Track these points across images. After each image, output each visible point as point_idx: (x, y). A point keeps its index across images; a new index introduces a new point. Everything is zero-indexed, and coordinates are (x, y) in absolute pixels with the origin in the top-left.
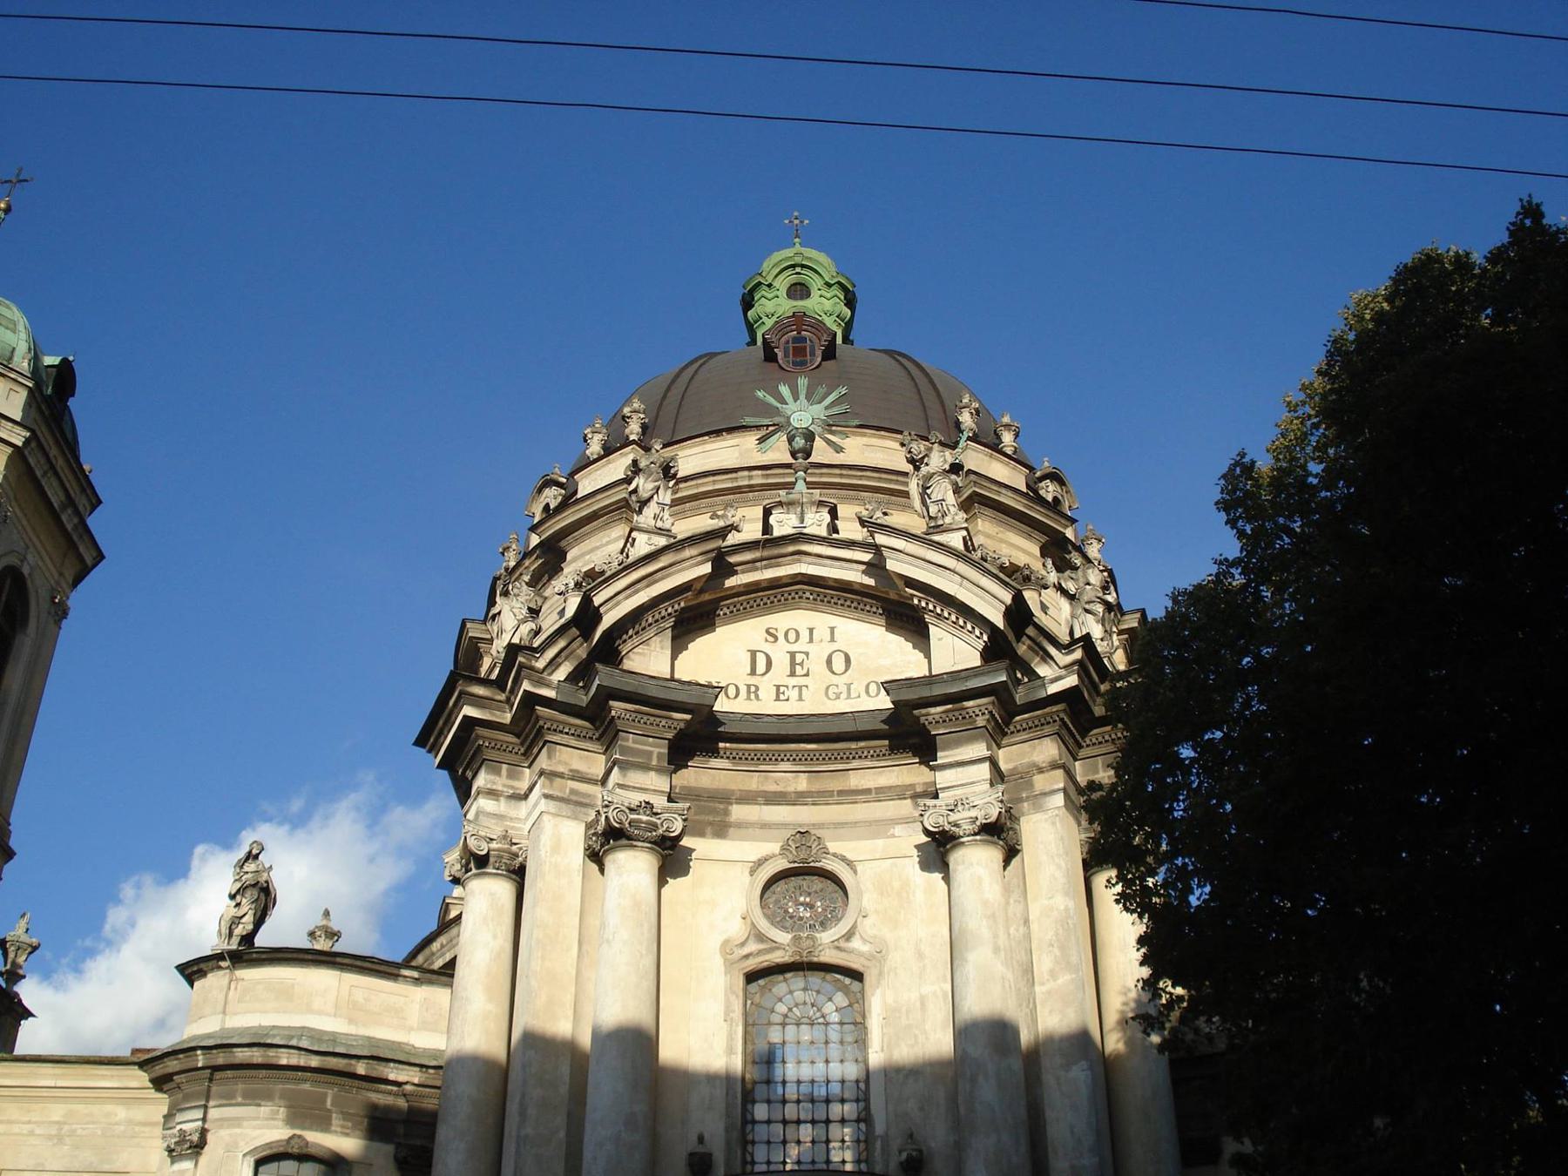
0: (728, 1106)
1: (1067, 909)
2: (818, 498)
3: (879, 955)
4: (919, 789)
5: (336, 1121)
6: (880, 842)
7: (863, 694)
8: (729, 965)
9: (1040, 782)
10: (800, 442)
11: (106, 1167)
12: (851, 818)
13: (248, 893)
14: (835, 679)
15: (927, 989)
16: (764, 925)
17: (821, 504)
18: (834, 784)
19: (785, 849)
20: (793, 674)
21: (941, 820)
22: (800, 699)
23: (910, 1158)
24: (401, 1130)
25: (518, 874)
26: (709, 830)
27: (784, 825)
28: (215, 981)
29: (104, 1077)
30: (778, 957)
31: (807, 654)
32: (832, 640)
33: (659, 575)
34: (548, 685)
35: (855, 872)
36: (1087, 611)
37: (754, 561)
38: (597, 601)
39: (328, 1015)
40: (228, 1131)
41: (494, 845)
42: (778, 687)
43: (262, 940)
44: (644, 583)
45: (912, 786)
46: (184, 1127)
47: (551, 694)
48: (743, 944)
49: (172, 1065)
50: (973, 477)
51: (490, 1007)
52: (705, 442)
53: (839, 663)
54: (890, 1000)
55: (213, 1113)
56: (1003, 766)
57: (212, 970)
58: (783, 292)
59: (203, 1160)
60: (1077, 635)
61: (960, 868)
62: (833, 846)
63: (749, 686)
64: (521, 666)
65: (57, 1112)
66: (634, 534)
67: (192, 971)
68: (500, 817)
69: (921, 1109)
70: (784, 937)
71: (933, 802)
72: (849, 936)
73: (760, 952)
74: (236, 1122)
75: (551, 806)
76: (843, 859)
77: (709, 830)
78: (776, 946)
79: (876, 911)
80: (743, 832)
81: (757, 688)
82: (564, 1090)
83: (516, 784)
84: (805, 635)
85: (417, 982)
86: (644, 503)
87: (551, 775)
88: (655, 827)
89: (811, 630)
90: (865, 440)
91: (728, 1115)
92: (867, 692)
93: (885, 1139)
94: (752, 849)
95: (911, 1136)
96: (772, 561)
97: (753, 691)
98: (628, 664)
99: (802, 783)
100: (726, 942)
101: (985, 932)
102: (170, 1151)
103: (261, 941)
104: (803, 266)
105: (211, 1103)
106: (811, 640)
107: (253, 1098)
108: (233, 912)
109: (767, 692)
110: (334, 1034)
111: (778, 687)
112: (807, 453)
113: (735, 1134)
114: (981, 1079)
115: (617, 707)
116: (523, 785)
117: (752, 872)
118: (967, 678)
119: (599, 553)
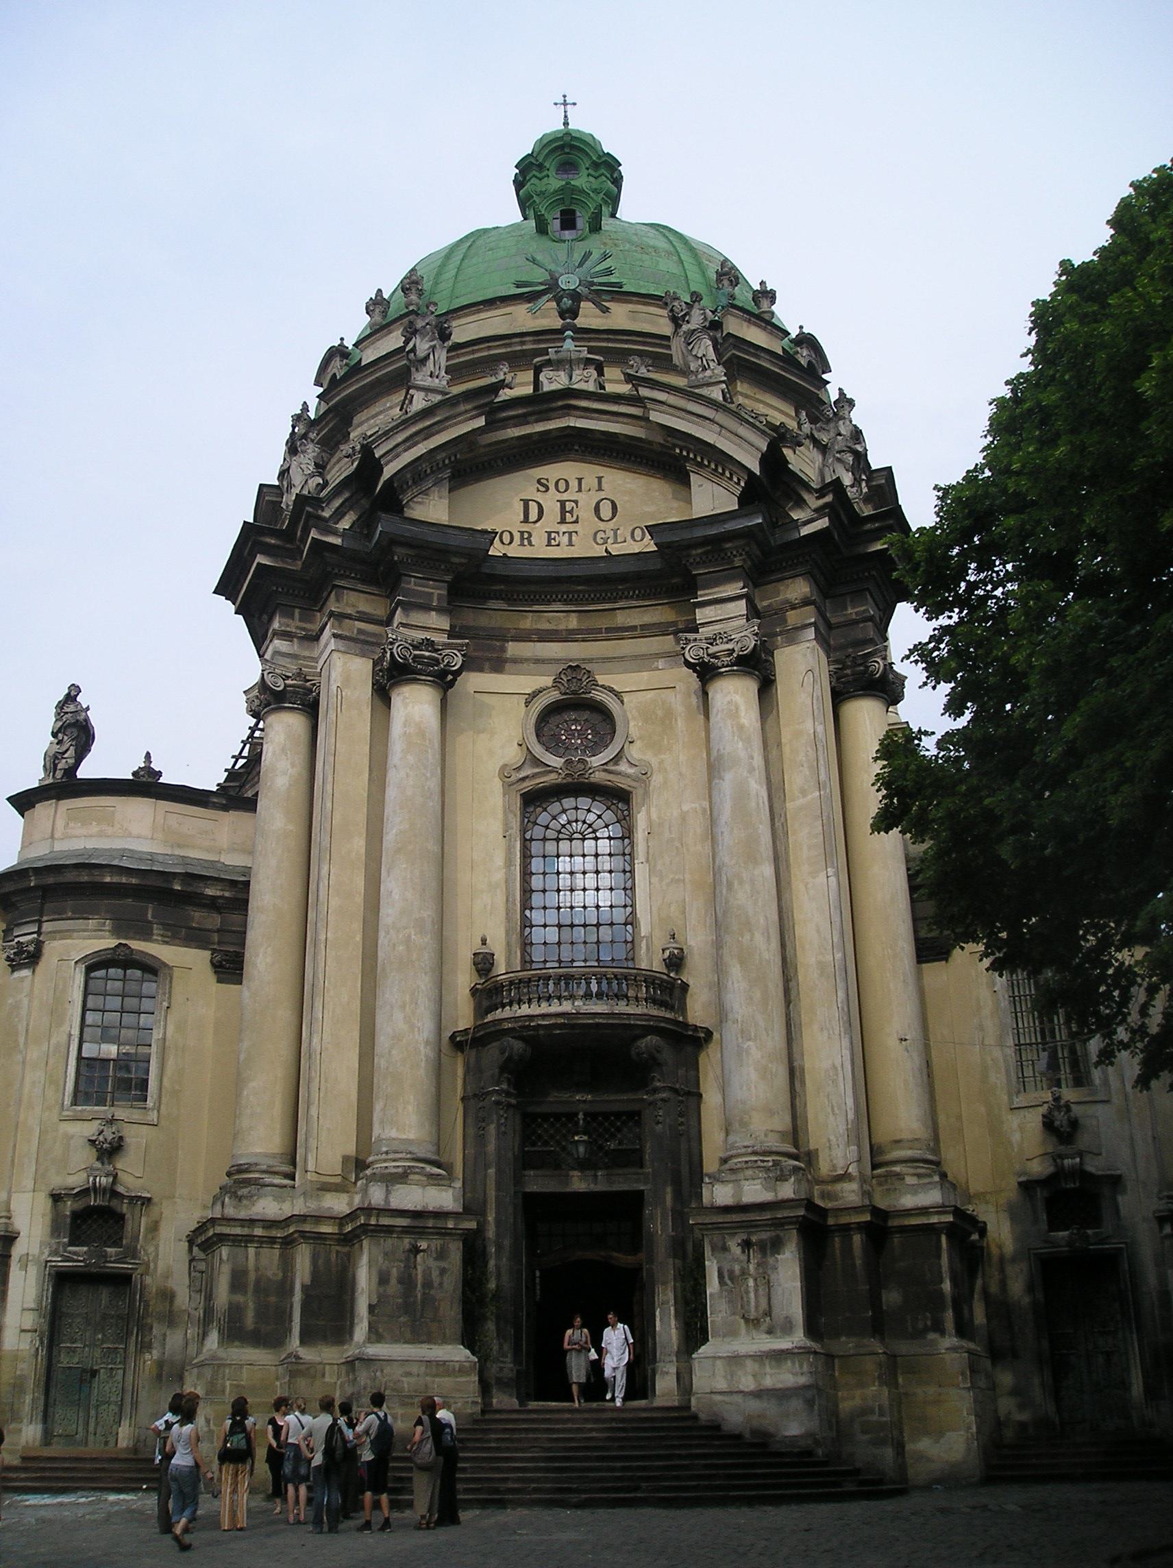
2: (585, 354)
5: (157, 930)
7: (629, 538)
8: (508, 786)
9: (793, 617)
10: (567, 302)
13: (69, 731)
14: (602, 525)
15: (685, 808)
16: (538, 750)
17: (588, 362)
18: (603, 622)
20: (563, 521)
22: (570, 544)
23: (672, 954)
24: (216, 937)
25: (311, 708)
26: (487, 665)
27: (557, 661)
28: (43, 810)
30: (551, 778)
31: (576, 502)
32: (600, 489)
33: (436, 428)
34: (334, 533)
35: (622, 702)
36: (839, 460)
37: (524, 415)
41: (289, 682)
42: (549, 533)
43: (82, 773)
44: (422, 436)
45: (674, 623)
46: (22, 939)
47: (337, 541)
50: (731, 340)
51: (290, 827)
52: (479, 311)
53: (606, 511)
54: (654, 816)
55: (46, 927)
56: (762, 604)
58: (552, 172)
59: (41, 968)
60: (828, 480)
62: (601, 679)
63: (522, 533)
64: (309, 515)
67: (23, 802)
68: (294, 657)
70: (556, 762)
71: (691, 636)
72: (616, 759)
73: (534, 776)
75: (341, 645)
76: (611, 690)
77: (487, 665)
79: (640, 738)
80: (519, 666)
81: (530, 535)
82: (359, 899)
83: (308, 626)
84: (574, 484)
85: (225, 808)
87: (340, 617)
88: (437, 662)
89: (580, 480)
90: (631, 307)
91: (508, 918)
92: (633, 537)
93: (649, 938)
94: (527, 683)
95: (673, 937)
96: (544, 416)
97: (526, 538)
98: (409, 513)
99: (573, 622)
100: (505, 766)
101: (742, 754)
102: (8, 959)
103: (82, 773)
104: (573, 147)
105: (45, 918)
106: (580, 490)
107: (82, 914)
108: (56, 748)
109: (539, 539)
110: (151, 854)
111: (549, 533)
112: (574, 313)
113: (515, 938)
116: (317, 627)
117: (527, 703)
118: (724, 521)
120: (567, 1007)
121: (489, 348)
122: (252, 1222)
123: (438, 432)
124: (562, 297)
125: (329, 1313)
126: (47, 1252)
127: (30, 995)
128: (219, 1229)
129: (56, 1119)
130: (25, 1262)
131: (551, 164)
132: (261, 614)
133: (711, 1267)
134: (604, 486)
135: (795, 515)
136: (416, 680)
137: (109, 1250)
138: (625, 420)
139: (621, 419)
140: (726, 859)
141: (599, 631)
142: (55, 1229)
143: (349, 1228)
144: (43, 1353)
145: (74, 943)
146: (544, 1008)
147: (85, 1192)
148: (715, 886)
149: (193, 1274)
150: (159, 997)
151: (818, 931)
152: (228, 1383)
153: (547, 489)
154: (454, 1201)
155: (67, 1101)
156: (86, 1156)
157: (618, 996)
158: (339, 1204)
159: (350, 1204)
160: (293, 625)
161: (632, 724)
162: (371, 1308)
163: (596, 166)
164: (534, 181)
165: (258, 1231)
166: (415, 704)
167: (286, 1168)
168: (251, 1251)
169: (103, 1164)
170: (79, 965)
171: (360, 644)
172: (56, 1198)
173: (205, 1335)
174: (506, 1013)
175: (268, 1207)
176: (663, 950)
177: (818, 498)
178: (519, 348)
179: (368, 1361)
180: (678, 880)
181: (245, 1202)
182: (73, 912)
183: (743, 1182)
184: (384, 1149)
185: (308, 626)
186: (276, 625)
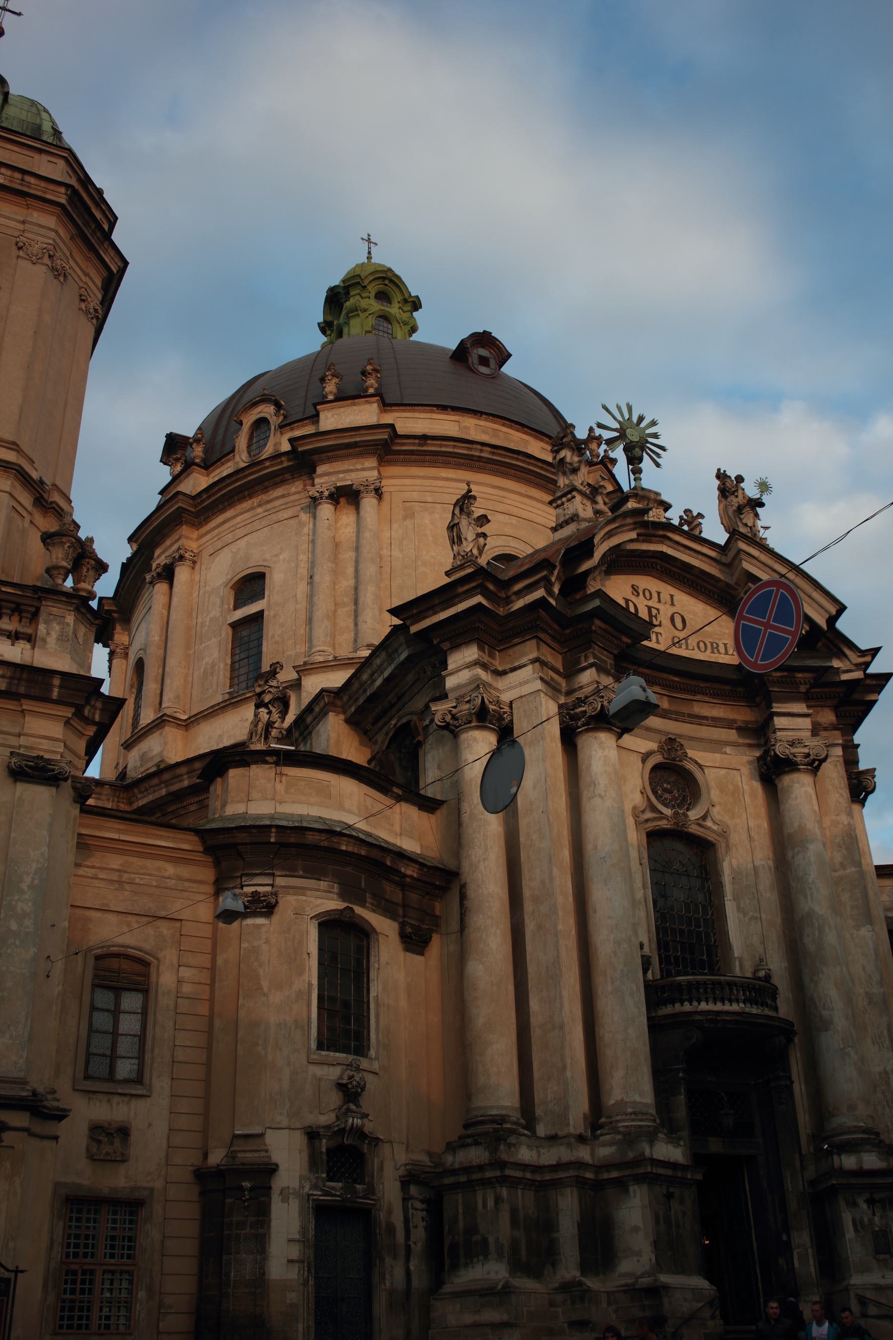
0: (648, 926)
1: (849, 824)
3: (724, 834)
4: (739, 724)
6: (717, 755)
7: (696, 648)
11: (163, 914)
12: (698, 735)
14: (677, 633)
18: (685, 709)
19: (661, 749)
21: (787, 751)
22: (658, 642)
24: (400, 911)
27: (658, 731)
29: (161, 838)
30: (664, 824)
32: (673, 604)
33: (614, 532)
38: (596, 541)
39: (354, 814)
40: (295, 897)
45: (734, 721)
46: (261, 889)
47: (553, 602)
48: (643, 812)
49: (242, 837)
52: (432, 412)
53: (679, 624)
57: (256, 763)
58: (372, 295)
59: (275, 918)
61: (796, 785)
62: (691, 753)
65: (115, 861)
66: (574, 493)
69: (763, 943)
70: (668, 812)
72: (704, 818)
73: (654, 819)
74: (301, 890)
76: (696, 762)
78: (663, 817)
79: (720, 804)
83: (493, 662)
84: (655, 595)
86: (575, 471)
87: (544, 664)
89: (659, 593)
91: (649, 930)
92: (699, 648)
93: (740, 959)
100: (635, 808)
104: (391, 281)
105: (277, 873)
106: (659, 601)
113: (654, 945)
114: (827, 929)
115: (597, 622)
117: (644, 761)
119: (353, 475)
120: (735, 1007)
121: (455, 447)
122: (525, 1167)
123: (614, 535)
124: (634, 447)
125: (599, 1245)
126: (308, 1187)
127: (267, 942)
128: (508, 1172)
129: (305, 1062)
130: (285, 1194)
131: (373, 289)
132: (441, 642)
133: (847, 1217)
134: (675, 602)
135: (836, 663)
136: (610, 730)
137: (358, 1186)
138: (704, 559)
139: (700, 557)
140: (817, 909)
141: (683, 714)
142: (313, 1162)
143: (614, 1174)
144: (311, 1282)
145: (310, 901)
146: (719, 1007)
147: (342, 1131)
148: (793, 926)
149: (411, 1211)
150: (372, 959)
151: (864, 970)
152: (525, 1309)
153: (638, 595)
154: (684, 1156)
155: (314, 1045)
156: (334, 1099)
157: (764, 1004)
158: (584, 1153)
159: (593, 1154)
160: (486, 659)
161: (713, 792)
162: (655, 1244)
163: (405, 301)
164: (358, 297)
165: (528, 1175)
166: (601, 751)
167: (522, 1121)
168: (519, 1192)
169: (356, 1105)
170: (314, 921)
171: (552, 687)
172: (312, 1135)
173: (455, 1267)
174: (687, 1007)
175: (525, 1154)
176: (756, 971)
177: (860, 656)
178: (478, 454)
179: (666, 1287)
180: (756, 918)
181: (512, 1149)
182: (304, 871)
183: (862, 1154)
184: (630, 1110)
185: (493, 662)
186: (471, 653)
